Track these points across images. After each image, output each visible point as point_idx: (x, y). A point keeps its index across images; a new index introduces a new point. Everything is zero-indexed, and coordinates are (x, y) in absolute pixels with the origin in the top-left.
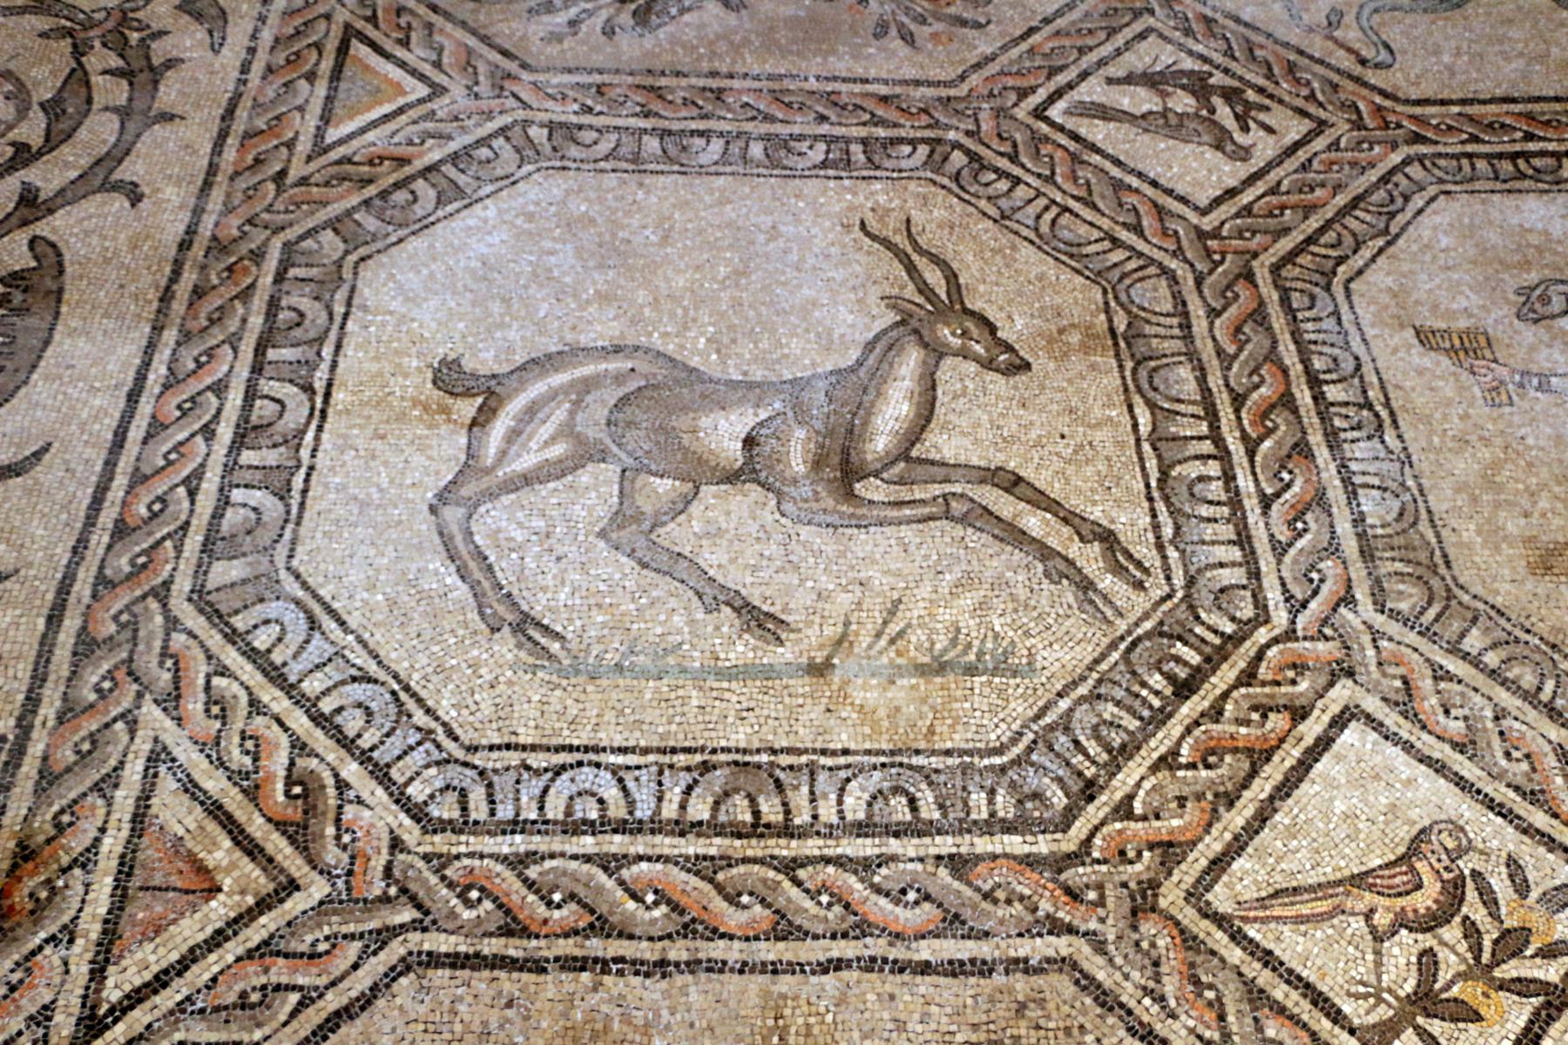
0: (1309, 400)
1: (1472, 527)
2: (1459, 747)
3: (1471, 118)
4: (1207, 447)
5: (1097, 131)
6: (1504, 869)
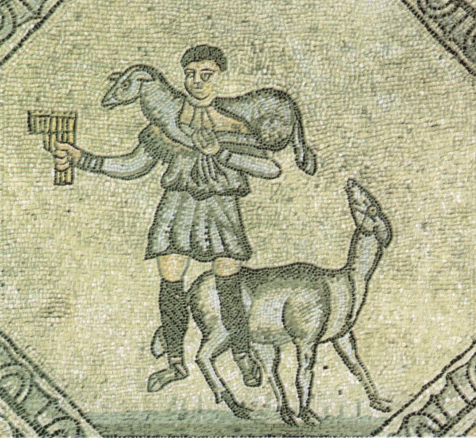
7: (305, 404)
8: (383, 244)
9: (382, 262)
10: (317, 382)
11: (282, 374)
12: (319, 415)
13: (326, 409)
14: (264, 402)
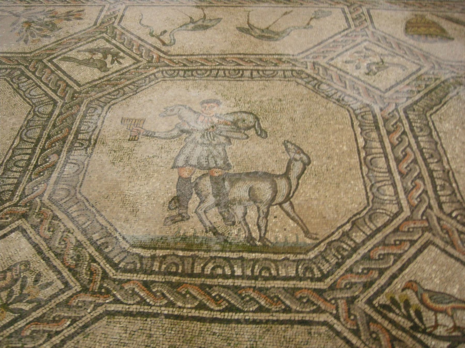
0: (72, 138)
1: (97, 176)
2: (45, 240)
3: (187, 60)
4: (29, 151)
5: (64, 66)
6: (34, 276)
7: (262, 235)
8: (305, 166)
9: (306, 172)
10: (270, 224)
11: (248, 220)
12: (272, 241)
13: (276, 238)
14: (236, 233)
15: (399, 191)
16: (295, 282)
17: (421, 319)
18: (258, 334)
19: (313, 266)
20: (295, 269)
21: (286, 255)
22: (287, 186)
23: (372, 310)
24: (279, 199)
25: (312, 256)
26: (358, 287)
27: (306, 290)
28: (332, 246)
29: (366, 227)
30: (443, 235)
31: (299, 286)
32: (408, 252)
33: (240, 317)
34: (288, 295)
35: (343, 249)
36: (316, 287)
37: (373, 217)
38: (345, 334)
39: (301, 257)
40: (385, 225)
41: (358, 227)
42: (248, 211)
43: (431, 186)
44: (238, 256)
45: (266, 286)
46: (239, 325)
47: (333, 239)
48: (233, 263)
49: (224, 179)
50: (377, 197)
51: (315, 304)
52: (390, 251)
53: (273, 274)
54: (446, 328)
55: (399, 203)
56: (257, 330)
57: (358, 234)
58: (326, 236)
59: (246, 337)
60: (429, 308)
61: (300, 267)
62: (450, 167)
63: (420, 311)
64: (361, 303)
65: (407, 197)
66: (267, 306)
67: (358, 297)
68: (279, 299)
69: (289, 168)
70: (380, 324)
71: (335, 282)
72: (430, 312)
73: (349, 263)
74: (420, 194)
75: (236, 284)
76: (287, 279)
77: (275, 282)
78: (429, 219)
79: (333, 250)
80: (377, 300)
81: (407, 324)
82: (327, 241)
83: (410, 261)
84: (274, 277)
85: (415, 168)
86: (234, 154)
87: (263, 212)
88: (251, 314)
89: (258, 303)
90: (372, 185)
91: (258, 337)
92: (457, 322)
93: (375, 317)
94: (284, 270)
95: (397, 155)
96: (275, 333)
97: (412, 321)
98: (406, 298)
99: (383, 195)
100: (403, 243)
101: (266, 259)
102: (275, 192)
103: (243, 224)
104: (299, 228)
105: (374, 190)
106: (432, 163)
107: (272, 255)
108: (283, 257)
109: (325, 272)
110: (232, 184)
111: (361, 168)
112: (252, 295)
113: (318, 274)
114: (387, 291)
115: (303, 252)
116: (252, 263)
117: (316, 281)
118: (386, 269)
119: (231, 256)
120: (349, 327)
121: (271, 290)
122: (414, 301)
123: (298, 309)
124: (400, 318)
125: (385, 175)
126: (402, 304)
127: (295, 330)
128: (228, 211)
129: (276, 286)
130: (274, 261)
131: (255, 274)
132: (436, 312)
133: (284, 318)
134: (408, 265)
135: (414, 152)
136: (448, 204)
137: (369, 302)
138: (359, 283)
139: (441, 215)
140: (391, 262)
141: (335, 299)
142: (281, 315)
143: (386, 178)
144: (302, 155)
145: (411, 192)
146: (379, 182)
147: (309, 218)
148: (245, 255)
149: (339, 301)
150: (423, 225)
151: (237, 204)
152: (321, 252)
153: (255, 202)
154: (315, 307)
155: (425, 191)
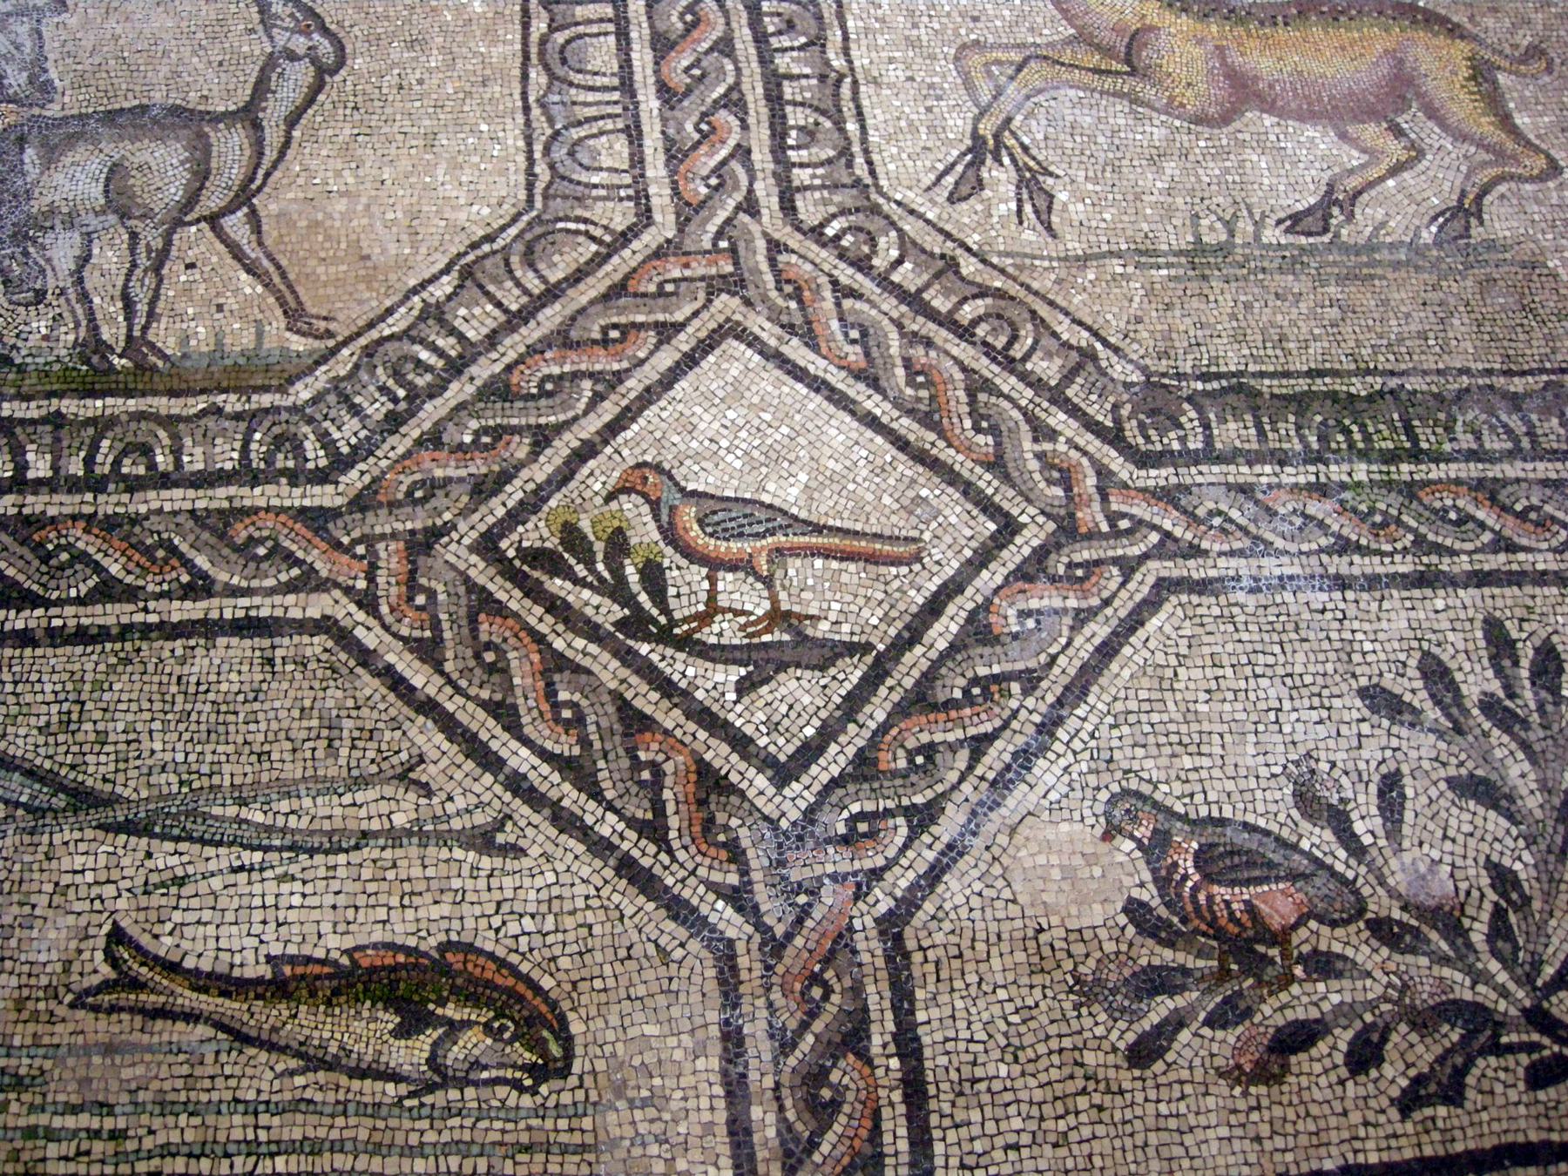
7: (137, 333)
8: (322, 73)
9: (321, 97)
10: (168, 292)
11: (92, 280)
12: (169, 352)
13: (185, 339)
15: (648, 151)
16: (232, 490)
17: (659, 595)
18: (89, 677)
19: (306, 429)
20: (237, 445)
21: (212, 399)
22: (248, 153)
23: (492, 571)
24: (212, 201)
25: (306, 395)
26: (453, 496)
27: (271, 515)
28: (377, 360)
29: (509, 284)
30: (780, 302)
31: (247, 503)
32: (647, 367)
33: (32, 624)
34: (206, 535)
35: (419, 363)
36: (307, 502)
37: (538, 248)
38: (391, 658)
39: (266, 400)
40: (578, 276)
41: (481, 287)
42: (96, 251)
43: (765, 133)
44: (44, 412)
45: (131, 509)
46: (28, 652)
47: (387, 332)
48: (22, 437)
49: (22, 141)
50: (563, 178)
51: (298, 563)
52: (583, 367)
53: (161, 468)
54: (742, 620)
55: (641, 198)
56: (88, 661)
57: (477, 311)
58: (361, 323)
59: (48, 688)
60: (691, 554)
61: (257, 436)
62: (850, 62)
63: (660, 565)
64: (457, 552)
65: (673, 172)
66: (129, 579)
67: (450, 527)
68: (173, 550)
69: (261, 88)
70: (516, 615)
71: (374, 480)
72: (694, 568)
73: (432, 411)
74: (724, 163)
75: (26, 511)
76: (208, 479)
77: (165, 494)
78: (741, 246)
79: (380, 370)
80: (515, 537)
81: (608, 613)
82: (363, 341)
83: (648, 397)
84: (165, 475)
85: (722, 69)
86: (69, 47)
87: (149, 250)
88: (69, 610)
89: (98, 568)
90: (556, 134)
91: (88, 687)
92: (783, 596)
93: (501, 596)
94: (198, 451)
95: (661, 26)
96: (151, 668)
97: (627, 599)
98: (616, 523)
99: (587, 169)
100: (631, 337)
101: (140, 416)
102: (201, 174)
103: (73, 297)
104: (271, 300)
105: (559, 153)
106: (784, 50)
107: (164, 400)
108: (201, 403)
109: (345, 450)
110: (50, 156)
111: (525, 77)
112: (80, 545)
113: (315, 456)
114: (553, 503)
115: (274, 382)
116: (91, 431)
117: (310, 481)
118: (560, 428)
119: (18, 415)
120: (405, 632)
121: (146, 524)
122: (645, 532)
123: (235, 581)
124: (586, 594)
125: (607, 97)
126: (599, 547)
127: (217, 655)
128: (26, 254)
129: (167, 507)
130: (170, 421)
131: (98, 470)
132: (714, 565)
133: (186, 616)
134: (641, 410)
135: (726, 14)
136: (817, 195)
137: (487, 546)
138: (461, 480)
139: (785, 234)
140: (581, 405)
141: (369, 540)
142: (176, 604)
143: (610, 110)
144: (316, 36)
145: (693, 155)
146: (580, 124)
147: (312, 262)
148: (69, 406)
149: (381, 546)
150: (713, 271)
151: (59, 227)
152: (337, 380)
153: (124, 215)
154: (295, 572)
155: (742, 152)
